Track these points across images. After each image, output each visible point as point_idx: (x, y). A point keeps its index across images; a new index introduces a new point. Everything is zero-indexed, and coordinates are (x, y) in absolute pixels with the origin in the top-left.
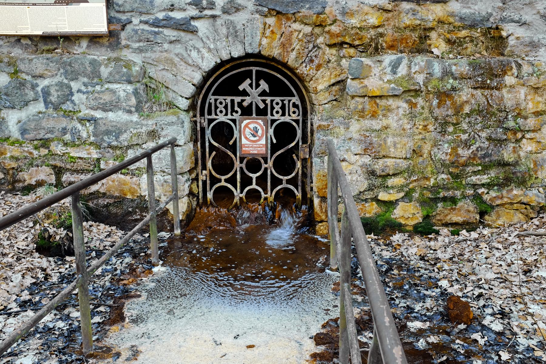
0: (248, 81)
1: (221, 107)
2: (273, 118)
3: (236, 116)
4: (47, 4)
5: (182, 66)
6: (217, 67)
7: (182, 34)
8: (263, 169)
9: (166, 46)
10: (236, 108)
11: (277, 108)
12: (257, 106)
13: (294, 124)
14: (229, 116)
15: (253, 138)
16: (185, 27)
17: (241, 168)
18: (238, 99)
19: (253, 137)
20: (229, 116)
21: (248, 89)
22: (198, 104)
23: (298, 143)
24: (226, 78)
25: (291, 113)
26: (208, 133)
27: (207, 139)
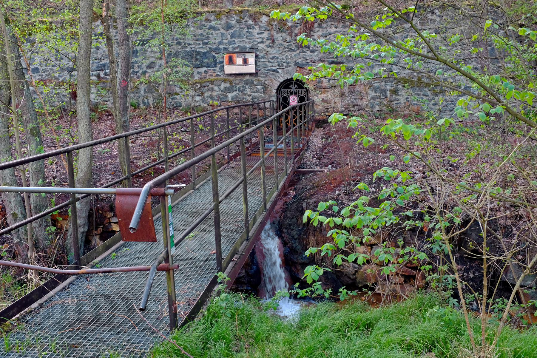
5: (275, 81)
16: (276, 71)
18: (289, 90)
19: (293, 101)
22: (278, 91)
24: (287, 84)
26: (281, 99)
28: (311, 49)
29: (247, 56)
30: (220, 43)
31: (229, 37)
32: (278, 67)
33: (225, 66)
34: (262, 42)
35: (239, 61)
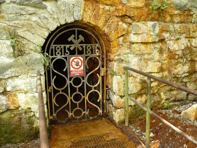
0: (73, 36)
1: (58, 51)
2: (87, 55)
3: (67, 55)
7: (37, 10)
9: (28, 16)
10: (67, 51)
11: (89, 50)
12: (78, 49)
13: (97, 58)
14: (63, 56)
15: (76, 67)
17: (70, 84)
18: (67, 46)
19: (76, 66)
20: (63, 56)
21: (73, 40)
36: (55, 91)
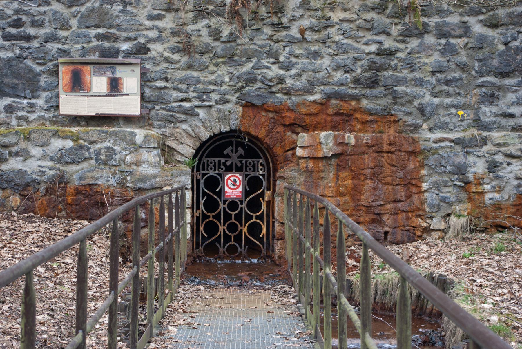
0: (230, 148)
1: (211, 165)
2: (246, 173)
3: (221, 171)
4: (100, 96)
6: (211, 138)
7: (188, 117)
8: (226, 225)
10: (222, 167)
11: (250, 166)
12: (236, 165)
13: (261, 177)
14: (217, 172)
15: (232, 187)
17: (224, 208)
18: (223, 160)
19: (233, 186)
20: (217, 172)
21: (230, 154)
23: (263, 191)
25: (259, 170)
26: (202, 183)
27: (201, 188)
28: (282, 59)
29: (121, 72)
30: (53, 38)
31: (74, 22)
32: (196, 103)
33: (62, 96)
34: (159, 39)
35: (99, 83)
36: (205, 217)
